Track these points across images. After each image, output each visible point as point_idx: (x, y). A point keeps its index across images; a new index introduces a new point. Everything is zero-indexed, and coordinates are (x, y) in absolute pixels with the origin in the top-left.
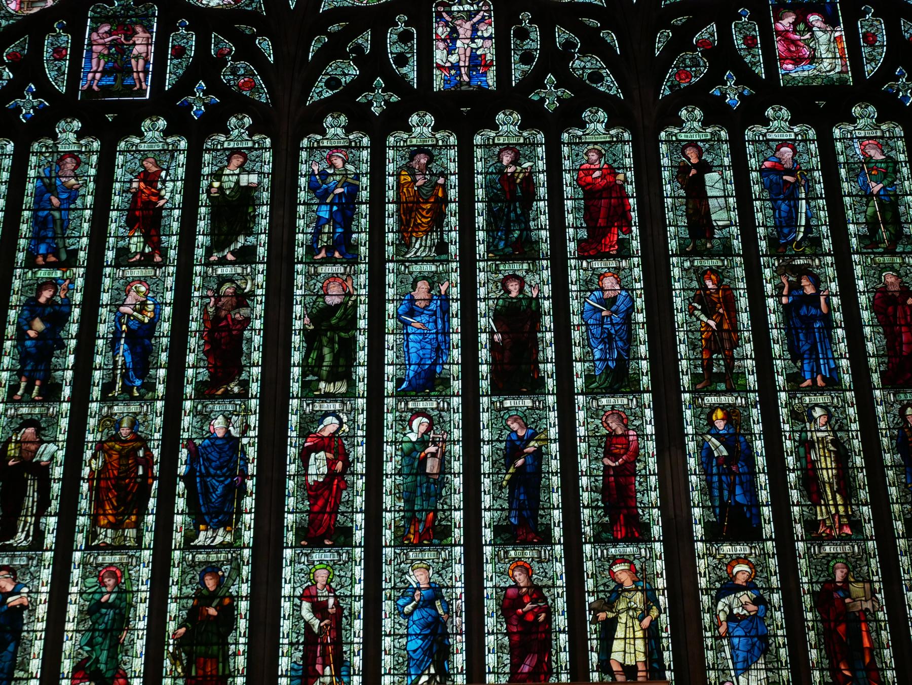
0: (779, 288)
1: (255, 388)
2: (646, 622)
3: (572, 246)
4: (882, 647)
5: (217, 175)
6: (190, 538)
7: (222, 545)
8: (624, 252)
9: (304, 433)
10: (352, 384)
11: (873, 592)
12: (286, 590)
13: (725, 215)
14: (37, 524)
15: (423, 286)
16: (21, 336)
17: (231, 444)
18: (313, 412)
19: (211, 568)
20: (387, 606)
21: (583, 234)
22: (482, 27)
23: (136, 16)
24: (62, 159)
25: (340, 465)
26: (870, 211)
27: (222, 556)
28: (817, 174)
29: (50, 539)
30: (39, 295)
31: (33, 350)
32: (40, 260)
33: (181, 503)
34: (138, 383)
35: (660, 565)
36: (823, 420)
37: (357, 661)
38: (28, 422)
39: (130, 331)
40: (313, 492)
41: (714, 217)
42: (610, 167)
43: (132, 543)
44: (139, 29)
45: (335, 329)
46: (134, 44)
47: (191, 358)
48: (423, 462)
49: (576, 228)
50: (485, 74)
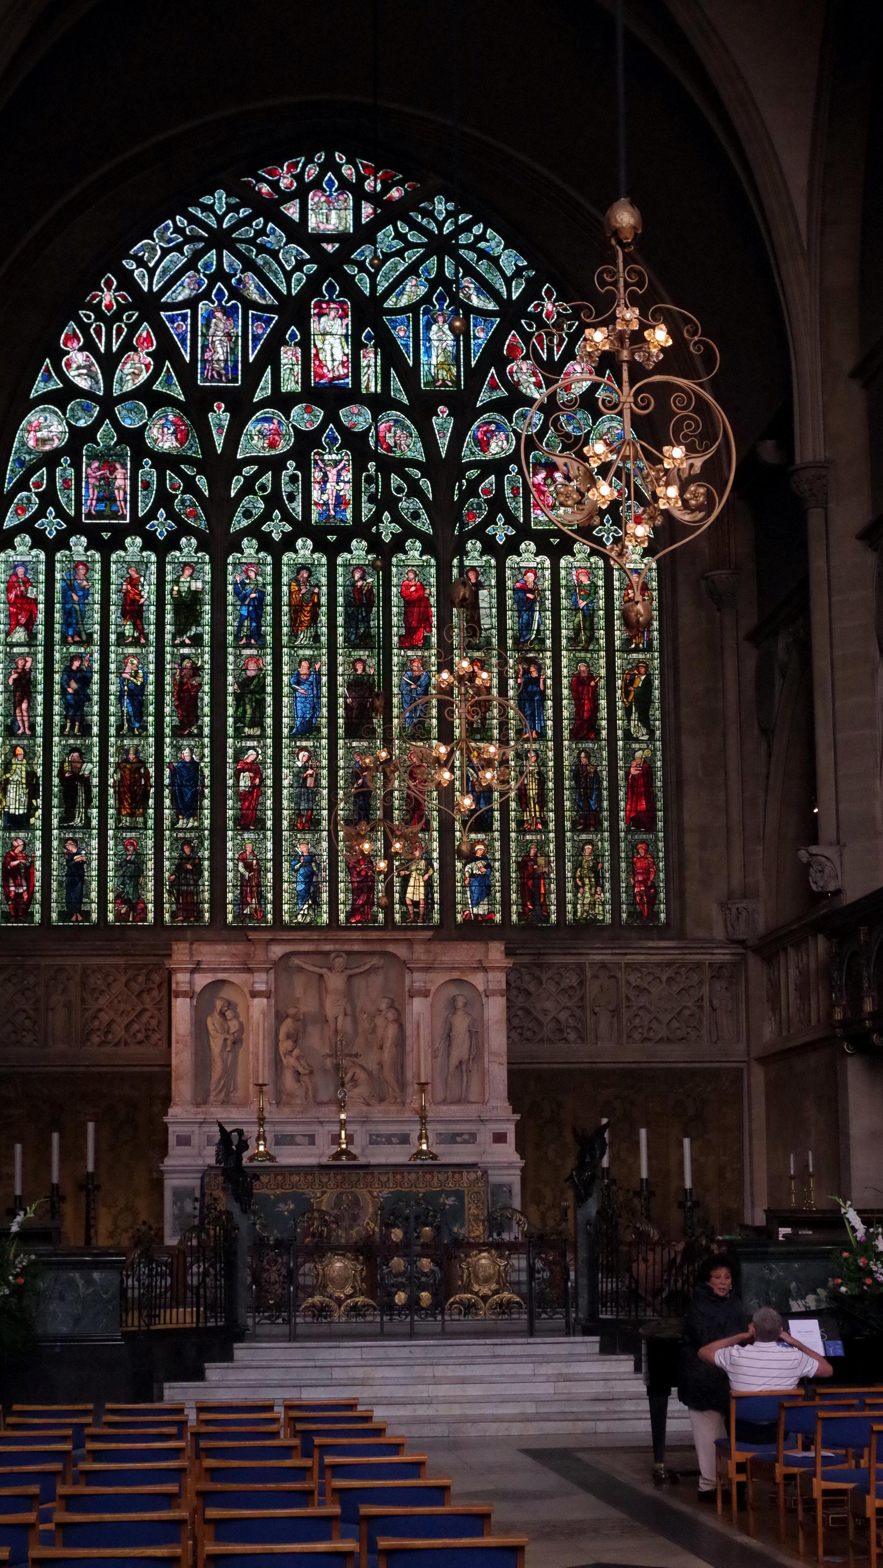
0: (517, 672)
1: (207, 731)
2: (426, 877)
3: (395, 639)
4: (550, 893)
5: (176, 582)
6: (174, 823)
7: (192, 828)
8: (427, 646)
9: (237, 760)
10: (263, 730)
11: (549, 862)
12: (230, 855)
13: (489, 621)
14: (86, 813)
15: (305, 664)
16: (64, 692)
17: (194, 766)
18: (241, 747)
19: (187, 842)
20: (286, 865)
21: (403, 631)
22: (344, 473)
23: (116, 455)
24: (76, 567)
25: (257, 781)
26: (577, 620)
27: (193, 835)
28: (548, 593)
29: (94, 822)
30: (72, 664)
31: (72, 702)
32: (70, 639)
33: (167, 802)
34: (137, 725)
35: (435, 845)
36: (534, 759)
37: (270, 896)
38: (74, 749)
39: (130, 690)
40: (241, 797)
41: (482, 622)
42: (422, 584)
43: (141, 826)
44: (118, 466)
45: (252, 692)
46: (116, 478)
47: (167, 710)
48: (305, 779)
49: (398, 627)
50: (344, 510)
